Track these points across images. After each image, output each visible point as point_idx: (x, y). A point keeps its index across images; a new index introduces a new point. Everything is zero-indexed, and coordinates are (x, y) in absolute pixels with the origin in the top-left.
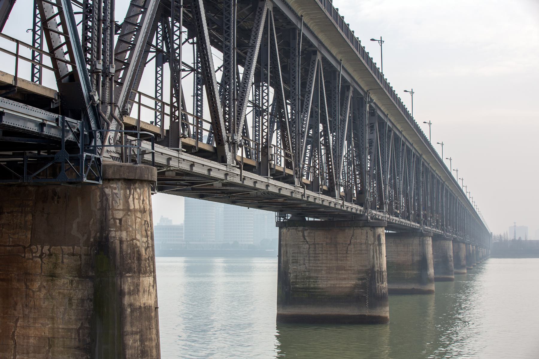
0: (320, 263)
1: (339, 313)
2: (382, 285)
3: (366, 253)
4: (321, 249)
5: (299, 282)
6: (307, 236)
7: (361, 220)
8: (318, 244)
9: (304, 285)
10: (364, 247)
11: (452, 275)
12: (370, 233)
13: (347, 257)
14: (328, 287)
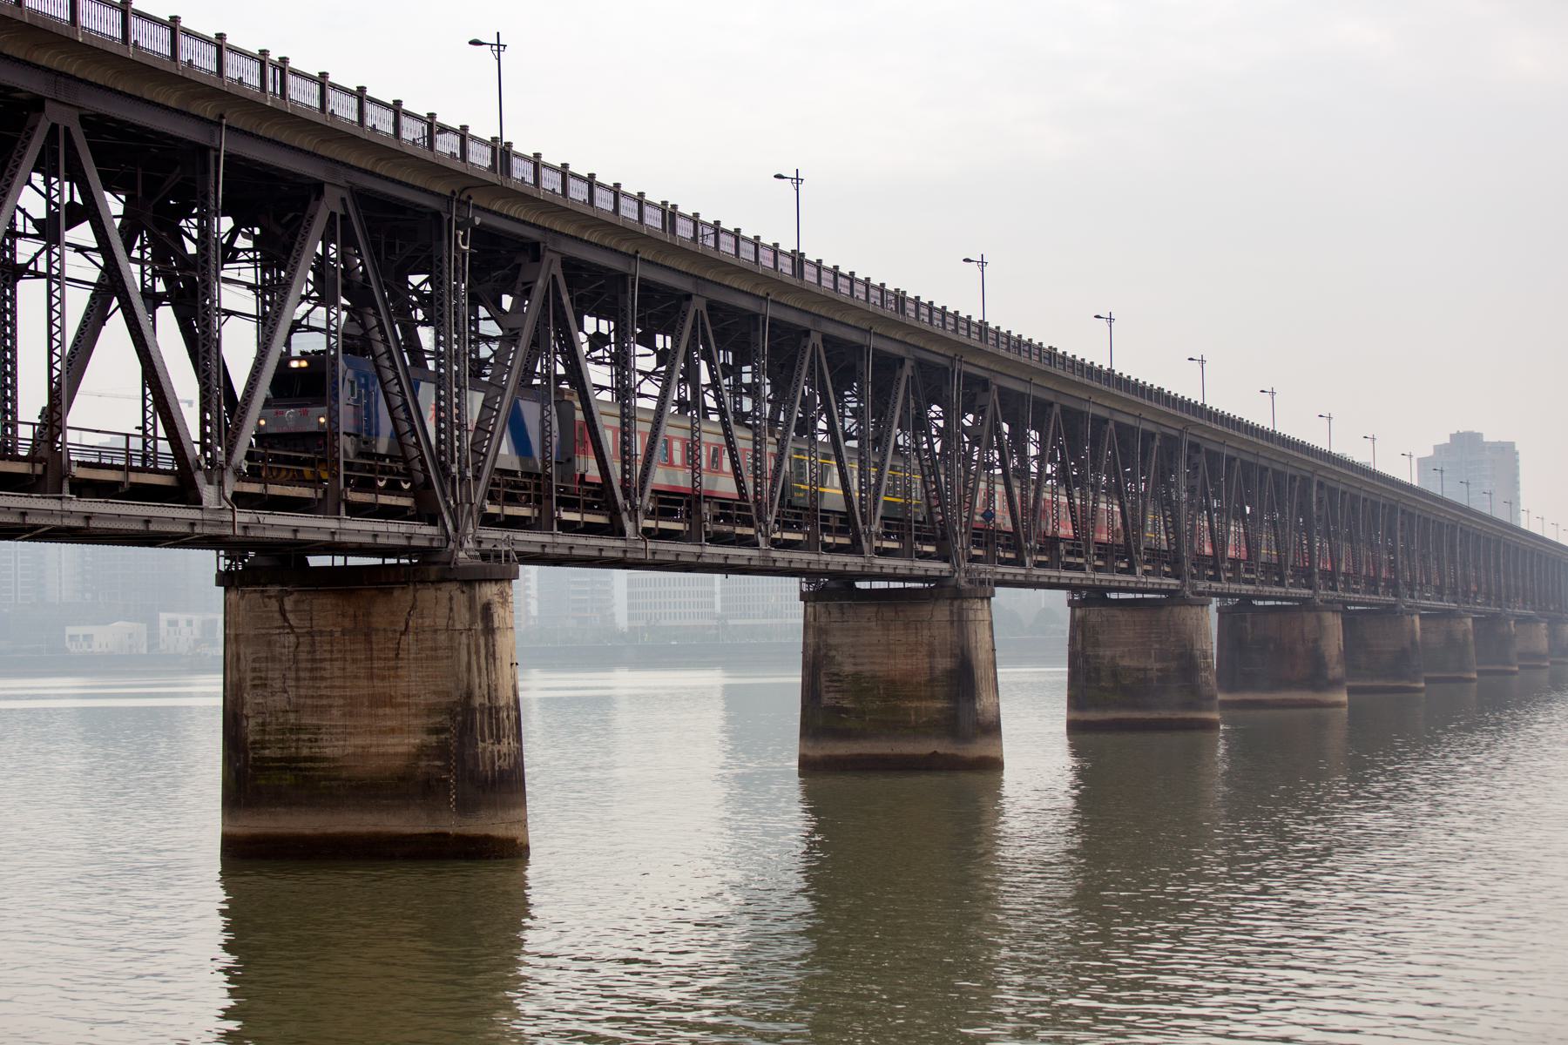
0: (326, 687)
1: (378, 829)
2: (497, 747)
3: (447, 657)
4: (327, 647)
5: (269, 741)
6: (291, 612)
7: (435, 563)
8: (321, 633)
9: (285, 751)
10: (442, 638)
11: (1210, 709)
12: (461, 599)
13: (397, 668)
14: (348, 755)
